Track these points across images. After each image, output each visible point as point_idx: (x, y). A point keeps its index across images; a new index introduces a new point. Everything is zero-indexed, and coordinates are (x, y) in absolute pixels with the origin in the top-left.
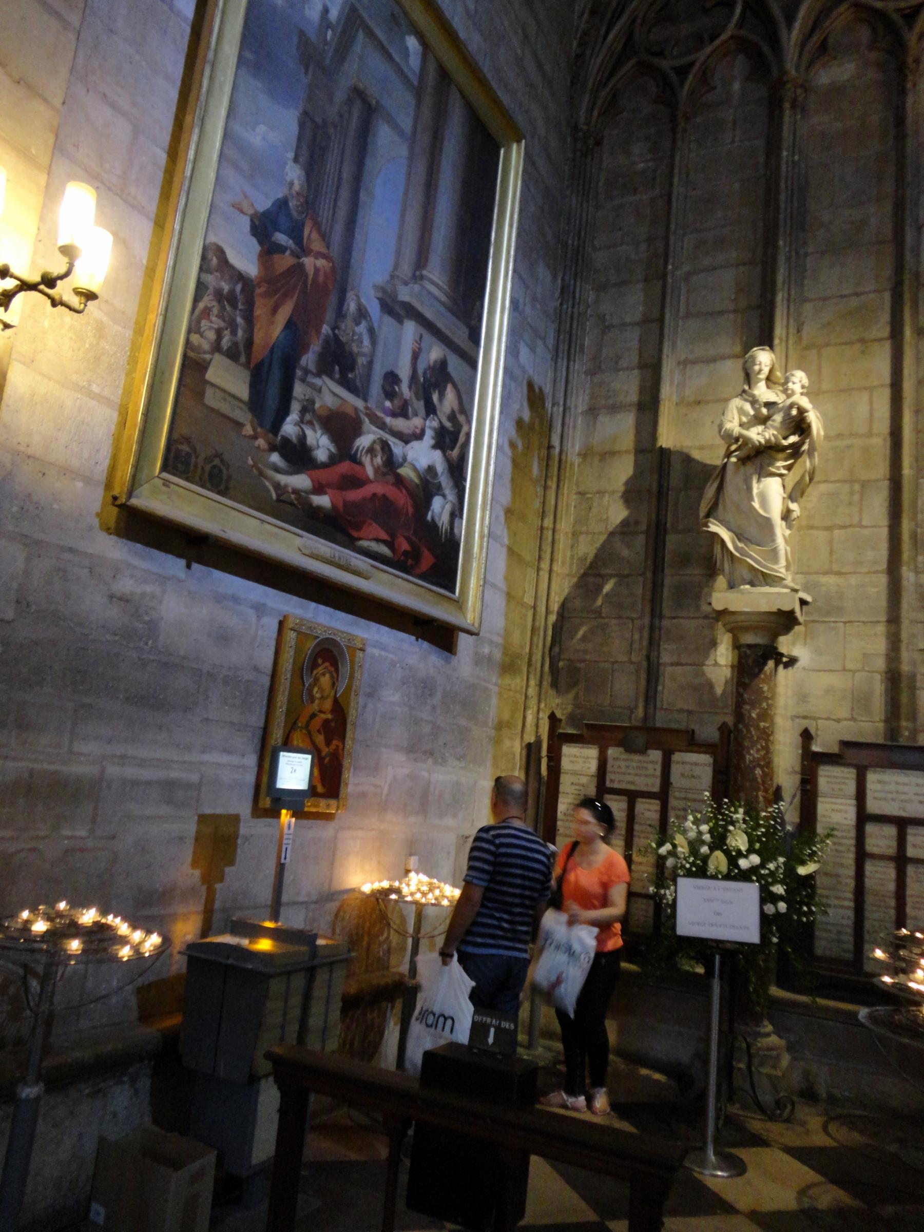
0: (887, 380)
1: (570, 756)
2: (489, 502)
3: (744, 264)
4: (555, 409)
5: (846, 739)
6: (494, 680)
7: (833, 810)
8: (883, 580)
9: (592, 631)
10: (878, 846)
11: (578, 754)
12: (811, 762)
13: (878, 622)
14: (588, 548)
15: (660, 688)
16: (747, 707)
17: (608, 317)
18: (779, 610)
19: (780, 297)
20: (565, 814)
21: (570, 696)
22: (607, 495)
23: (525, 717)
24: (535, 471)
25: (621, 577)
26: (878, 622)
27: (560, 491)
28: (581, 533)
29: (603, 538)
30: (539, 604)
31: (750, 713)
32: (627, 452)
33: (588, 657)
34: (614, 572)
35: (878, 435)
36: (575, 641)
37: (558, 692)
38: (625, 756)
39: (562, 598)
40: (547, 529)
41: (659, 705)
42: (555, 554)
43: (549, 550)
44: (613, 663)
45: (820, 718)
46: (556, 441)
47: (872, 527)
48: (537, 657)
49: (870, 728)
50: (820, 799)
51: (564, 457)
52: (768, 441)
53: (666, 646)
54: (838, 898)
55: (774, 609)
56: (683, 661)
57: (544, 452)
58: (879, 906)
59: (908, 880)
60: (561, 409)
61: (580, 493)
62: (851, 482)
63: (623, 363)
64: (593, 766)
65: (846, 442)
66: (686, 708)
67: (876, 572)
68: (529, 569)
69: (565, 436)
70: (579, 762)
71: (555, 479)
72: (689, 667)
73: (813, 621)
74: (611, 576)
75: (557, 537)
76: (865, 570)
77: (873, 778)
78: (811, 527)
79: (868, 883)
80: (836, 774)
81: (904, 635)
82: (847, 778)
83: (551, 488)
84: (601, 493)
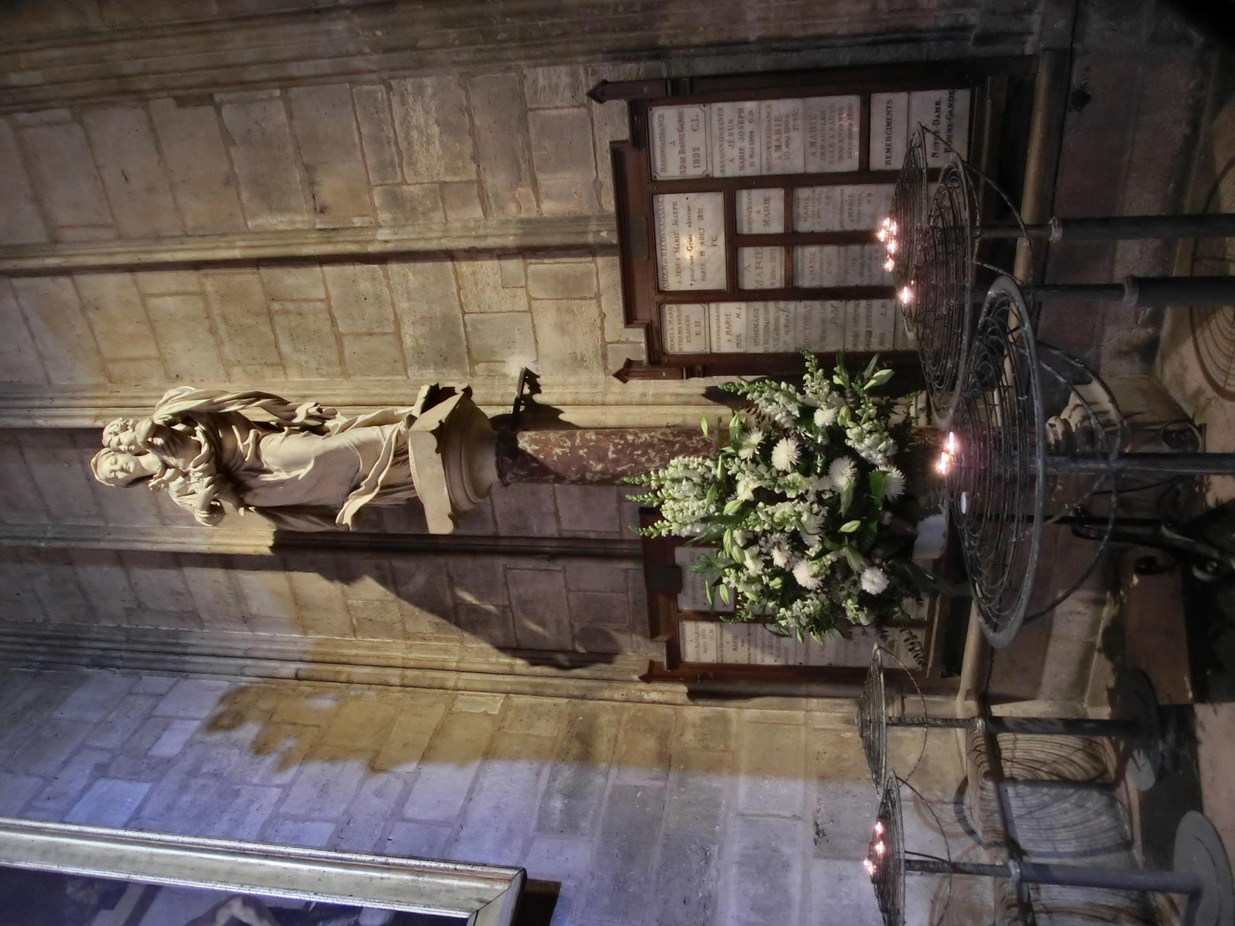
0: (126, 278)
1: (698, 653)
2: (340, 855)
3: (22, 454)
4: (247, 671)
5: (621, 318)
6: (599, 780)
7: (728, 333)
8: (394, 268)
9: (531, 615)
10: (773, 272)
11: (694, 644)
12: (659, 362)
13: (455, 271)
14: (424, 621)
15: (592, 536)
16: (589, 476)
17: (128, 605)
18: (437, 451)
19: (41, 423)
20: (778, 656)
21: (622, 639)
22: (350, 601)
23: (654, 702)
24: (325, 703)
25: (452, 585)
26: (455, 271)
27: (353, 660)
28: (404, 630)
29: (405, 604)
30: (502, 687)
31: (597, 473)
32: (290, 580)
33: (566, 621)
34: (448, 593)
35: (202, 284)
36: (547, 634)
37: (615, 653)
38: (688, 588)
39: (495, 651)
40: (403, 677)
41: (617, 537)
42: (434, 665)
43: (430, 674)
44: (569, 590)
45: (603, 339)
46: (289, 669)
47: (326, 287)
48: (571, 685)
49: (605, 273)
50: (715, 350)
51: (309, 658)
52: (206, 472)
53: (535, 530)
54: (856, 322)
55: (438, 457)
56: (553, 509)
57: (305, 687)
58: (862, 265)
59: (818, 229)
60: (249, 662)
61: (354, 632)
62: (270, 315)
63: (180, 587)
64: (707, 627)
65: (219, 320)
66: (615, 505)
67: (387, 276)
68: (459, 706)
69: (281, 656)
70: (702, 643)
71: (339, 668)
72: (558, 501)
73: (469, 353)
74: (455, 597)
75: (412, 664)
76: (386, 291)
77: (673, 283)
78: (342, 362)
79: (829, 282)
80: (676, 331)
81: (464, 244)
82: (679, 316)
83: (349, 674)
84: (348, 609)
